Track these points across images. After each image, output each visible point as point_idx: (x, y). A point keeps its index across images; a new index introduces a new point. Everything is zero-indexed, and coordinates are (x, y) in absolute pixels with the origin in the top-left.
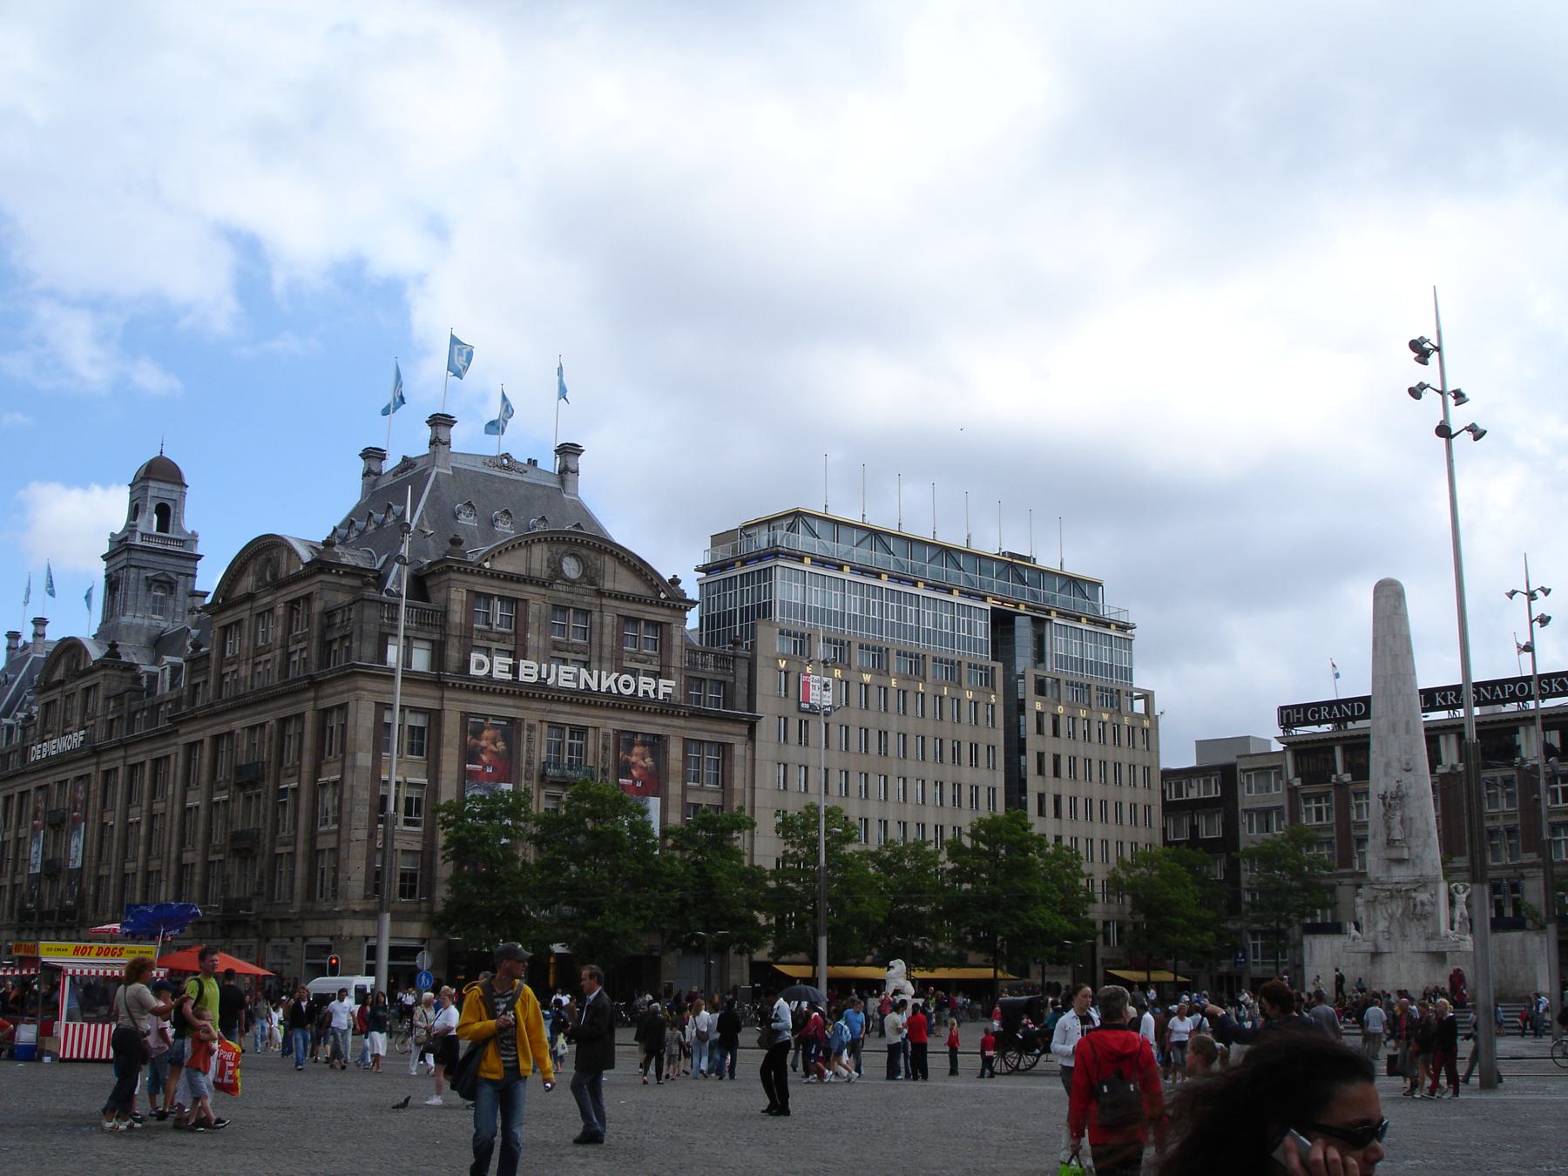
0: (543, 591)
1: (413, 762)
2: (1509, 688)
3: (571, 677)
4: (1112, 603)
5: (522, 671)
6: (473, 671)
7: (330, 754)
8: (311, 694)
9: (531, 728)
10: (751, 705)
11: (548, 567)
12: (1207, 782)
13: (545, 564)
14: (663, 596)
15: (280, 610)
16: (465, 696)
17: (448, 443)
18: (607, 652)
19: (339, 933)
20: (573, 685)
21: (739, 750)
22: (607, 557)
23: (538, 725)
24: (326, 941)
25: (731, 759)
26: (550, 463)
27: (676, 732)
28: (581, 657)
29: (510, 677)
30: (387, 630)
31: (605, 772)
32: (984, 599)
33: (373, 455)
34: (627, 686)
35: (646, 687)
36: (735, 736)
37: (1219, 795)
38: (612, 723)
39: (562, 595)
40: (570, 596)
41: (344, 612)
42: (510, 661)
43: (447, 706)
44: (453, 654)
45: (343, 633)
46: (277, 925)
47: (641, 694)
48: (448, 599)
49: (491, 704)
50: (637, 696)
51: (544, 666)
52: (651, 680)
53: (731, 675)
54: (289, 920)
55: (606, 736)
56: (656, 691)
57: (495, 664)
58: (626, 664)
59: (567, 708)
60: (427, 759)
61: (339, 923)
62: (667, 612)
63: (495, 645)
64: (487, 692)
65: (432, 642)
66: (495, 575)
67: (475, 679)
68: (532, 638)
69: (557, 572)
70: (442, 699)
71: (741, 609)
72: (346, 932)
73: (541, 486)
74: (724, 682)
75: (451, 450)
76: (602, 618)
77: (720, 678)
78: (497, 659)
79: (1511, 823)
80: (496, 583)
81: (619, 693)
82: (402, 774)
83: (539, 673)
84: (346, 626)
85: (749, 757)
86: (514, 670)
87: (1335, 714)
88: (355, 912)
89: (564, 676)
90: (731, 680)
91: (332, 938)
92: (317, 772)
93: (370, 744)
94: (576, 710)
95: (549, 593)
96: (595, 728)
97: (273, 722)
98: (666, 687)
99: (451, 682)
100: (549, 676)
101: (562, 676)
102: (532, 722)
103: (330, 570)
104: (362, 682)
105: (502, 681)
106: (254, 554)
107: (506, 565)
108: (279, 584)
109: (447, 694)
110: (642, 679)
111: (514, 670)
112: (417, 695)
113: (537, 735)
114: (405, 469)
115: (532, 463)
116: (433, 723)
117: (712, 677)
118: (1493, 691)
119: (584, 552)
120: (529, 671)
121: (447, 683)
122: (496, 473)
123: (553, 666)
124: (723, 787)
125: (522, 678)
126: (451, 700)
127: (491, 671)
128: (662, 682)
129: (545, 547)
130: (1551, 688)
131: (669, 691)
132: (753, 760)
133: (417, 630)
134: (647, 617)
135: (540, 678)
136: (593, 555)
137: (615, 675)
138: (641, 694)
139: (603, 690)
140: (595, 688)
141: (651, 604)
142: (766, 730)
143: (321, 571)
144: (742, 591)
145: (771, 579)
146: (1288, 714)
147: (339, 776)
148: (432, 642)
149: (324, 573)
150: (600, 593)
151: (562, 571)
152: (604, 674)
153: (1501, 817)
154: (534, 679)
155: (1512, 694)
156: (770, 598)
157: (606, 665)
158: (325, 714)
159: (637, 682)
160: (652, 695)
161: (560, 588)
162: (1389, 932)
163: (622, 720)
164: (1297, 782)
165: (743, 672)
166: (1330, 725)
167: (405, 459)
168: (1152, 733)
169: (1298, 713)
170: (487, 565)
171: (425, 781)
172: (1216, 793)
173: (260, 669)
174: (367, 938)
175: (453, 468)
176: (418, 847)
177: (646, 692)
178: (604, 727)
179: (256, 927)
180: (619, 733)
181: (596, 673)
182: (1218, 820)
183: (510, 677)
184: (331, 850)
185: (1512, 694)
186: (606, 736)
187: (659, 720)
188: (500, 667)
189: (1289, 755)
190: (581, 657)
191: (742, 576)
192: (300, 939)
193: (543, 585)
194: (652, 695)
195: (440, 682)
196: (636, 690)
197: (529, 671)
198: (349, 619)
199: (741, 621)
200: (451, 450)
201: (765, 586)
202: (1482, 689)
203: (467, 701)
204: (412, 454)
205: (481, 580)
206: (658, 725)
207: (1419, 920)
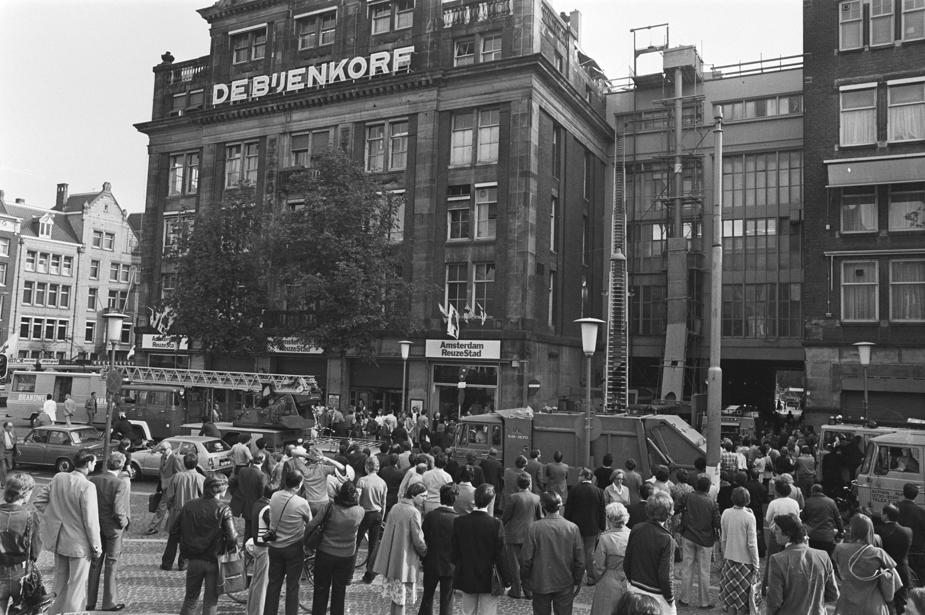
9: (273, 141)
34: (358, 68)
35: (379, 64)
51: (275, 76)
52: (386, 55)
55: (345, 131)
56: (390, 65)
83: (270, 85)
89: (292, 80)
96: (336, 126)
98: (402, 56)
100: (278, 84)
102: (273, 137)
117: (481, 29)
123: (283, 74)
137: (344, 61)
138: (373, 72)
140: (322, 80)
159: (368, 61)
160: (386, 70)
177: (379, 69)
178: (343, 122)
186: (345, 131)
190: (327, 58)
194: (386, 70)
197: (261, 86)
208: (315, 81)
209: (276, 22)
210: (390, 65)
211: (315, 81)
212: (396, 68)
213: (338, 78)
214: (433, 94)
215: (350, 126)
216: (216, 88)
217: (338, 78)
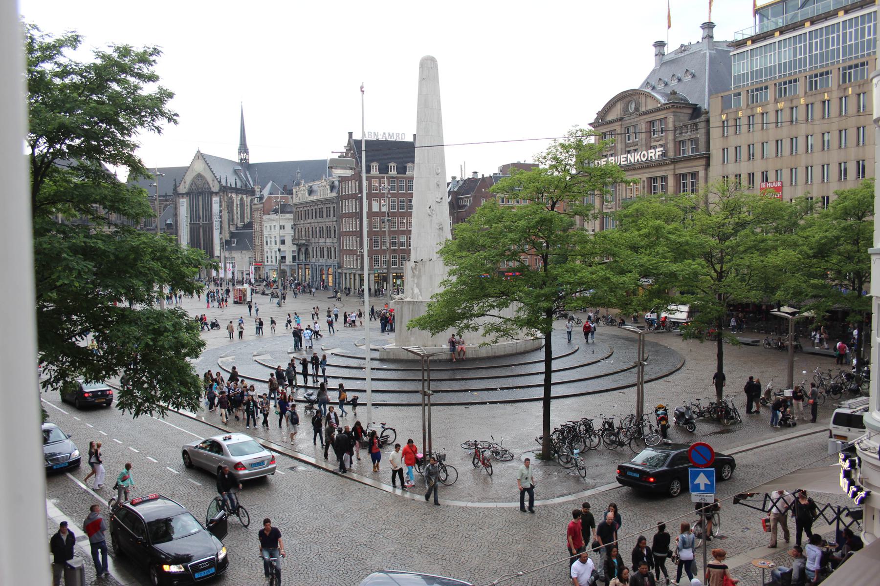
14: (659, 105)
20: (625, 163)
21: (702, 174)
27: (668, 171)
28: (636, 147)
34: (644, 156)
38: (645, 175)
47: (649, 159)
55: (644, 181)
62: (665, 112)
80: (606, 126)
94: (634, 172)
101: (622, 160)
134: (657, 118)
138: (649, 159)
160: (653, 157)
163: (650, 172)
177: (651, 157)
186: (644, 181)
206: (662, 171)
214: (672, 167)
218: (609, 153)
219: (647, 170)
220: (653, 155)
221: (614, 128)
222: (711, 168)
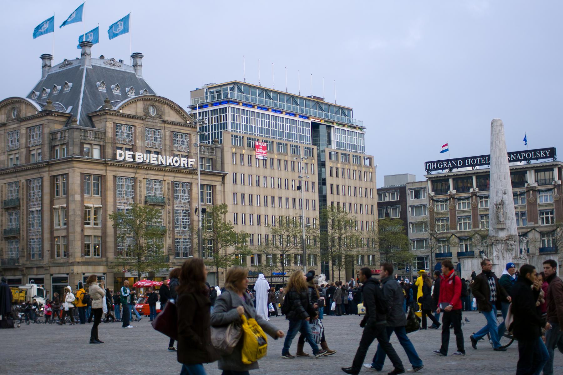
0: (142, 122)
1: (96, 198)
2: (523, 155)
3: (155, 159)
4: (356, 118)
5: (137, 157)
6: (118, 158)
7: (57, 195)
8: (47, 169)
9: (140, 181)
10: (223, 169)
11: (143, 111)
12: (393, 194)
13: (142, 110)
14: (188, 122)
15: (23, 131)
16: (117, 169)
17: (89, 55)
18: (167, 147)
19: (72, 272)
20: (156, 163)
21: (219, 188)
22: (166, 106)
23: (143, 180)
24: (65, 275)
25: (216, 192)
26: (129, 61)
28: (157, 150)
29: (132, 160)
30: (83, 141)
31: (169, 199)
32: (308, 118)
33: (46, 57)
34: (176, 162)
35: (184, 162)
36: (216, 181)
37: (398, 200)
38: (170, 178)
39: (149, 123)
40: (152, 124)
41: (61, 133)
42: (132, 153)
43: (108, 173)
44: (109, 151)
45: (62, 142)
46: (35, 270)
47: (182, 165)
48: (105, 126)
49: (125, 172)
50: (180, 166)
52: (186, 159)
53: (214, 155)
54: (42, 267)
55: (168, 183)
56: (188, 164)
57: (127, 155)
58: (175, 153)
59: (153, 172)
60: (101, 196)
61: (71, 267)
62: (189, 129)
63: (124, 146)
64: (124, 167)
65: (100, 145)
66: (124, 116)
67: (119, 161)
68: (139, 143)
69: (147, 114)
70: (106, 170)
71: (212, 126)
72: (75, 271)
73: (127, 72)
74: (212, 159)
75: (92, 57)
76: (165, 133)
77: (211, 157)
78: (127, 152)
79: (523, 210)
81: (174, 165)
82: (92, 203)
83: (143, 158)
84: (64, 139)
85: (222, 191)
86: (133, 157)
87: (450, 165)
88: (78, 263)
89: (152, 159)
90: (215, 157)
91: (68, 274)
92: (52, 203)
93: (79, 191)
94: (157, 173)
95: (145, 122)
97: (24, 181)
98: (191, 162)
99: (110, 163)
102: (140, 179)
103: (52, 114)
104: (75, 164)
105: (130, 162)
106: (5, 105)
107: (127, 111)
108: (21, 120)
109: (108, 168)
110: (182, 159)
111: (133, 157)
112: (96, 169)
113: (142, 184)
114: (67, 65)
115: (121, 61)
116: (102, 181)
117: (207, 157)
118: (517, 156)
119: (157, 104)
120: (140, 157)
121: (108, 163)
122: (108, 67)
124: (213, 204)
125: (137, 160)
126: (110, 170)
127: (125, 158)
128: (190, 160)
129: (142, 102)
130: (541, 155)
131: (193, 163)
132: (224, 192)
133: (95, 141)
135: (143, 160)
136: (160, 105)
137: (172, 157)
138: (182, 165)
139: (168, 164)
140: (164, 163)
141: (184, 126)
142: (229, 179)
143: (48, 115)
144: (212, 118)
145: (226, 112)
146: (429, 165)
147: (65, 205)
148: (100, 145)
149: (49, 115)
150: (164, 122)
151: (149, 113)
152: (168, 157)
153: (519, 208)
154: (141, 161)
155: (525, 157)
156: (226, 120)
157: (168, 153)
158: (54, 178)
160: (186, 166)
161: (148, 120)
162: (498, 257)
164: (433, 194)
165: (219, 154)
166: (447, 170)
167: (65, 60)
168: (373, 174)
169: (434, 165)
170: (121, 111)
171: (101, 206)
172: (397, 199)
173: (12, 157)
174: (84, 274)
175: (92, 66)
176: (100, 234)
177: (184, 164)
179: (22, 271)
180: (173, 182)
181: (164, 157)
182: (399, 210)
183: (132, 160)
184: (64, 237)
185: (525, 157)
186: (168, 183)
187: (191, 176)
188: (127, 156)
189: (429, 183)
191: (211, 111)
192: (49, 275)
193: (142, 120)
195: (106, 163)
196: (180, 164)
197: (139, 157)
198: (65, 137)
199: (212, 131)
200: (92, 57)
201: (224, 116)
202: (512, 155)
203: (116, 171)
204: (69, 58)
205: (118, 118)
206: (188, 178)
207: (510, 251)
208: (161, 162)
209: (138, 127)
210: (188, 165)
211: (161, 162)
212: (189, 166)
213: (170, 163)
215: (171, 182)
216: (119, 152)
217: (170, 163)
218: (124, 146)
219: (173, 174)
220: (186, 163)
221: (135, 124)
222: (226, 185)
